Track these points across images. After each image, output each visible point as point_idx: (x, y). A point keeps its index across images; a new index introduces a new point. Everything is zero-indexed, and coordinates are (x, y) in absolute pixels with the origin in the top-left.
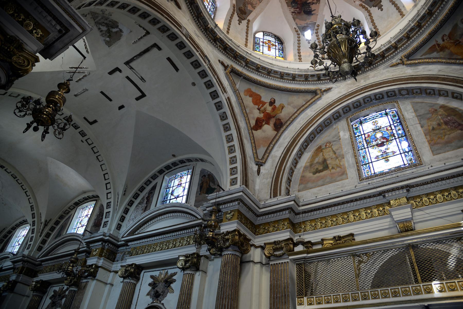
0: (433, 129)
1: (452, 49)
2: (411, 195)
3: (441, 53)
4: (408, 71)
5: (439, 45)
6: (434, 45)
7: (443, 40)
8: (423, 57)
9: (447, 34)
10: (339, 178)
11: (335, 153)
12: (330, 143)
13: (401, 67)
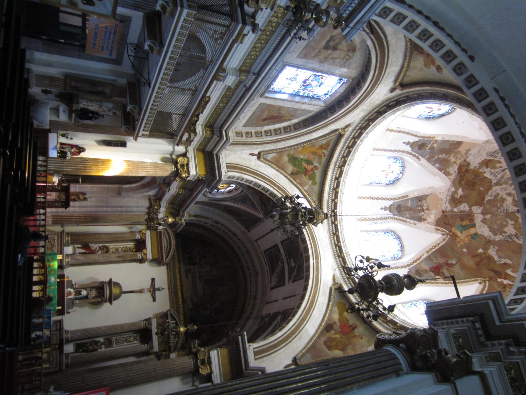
0: (280, 110)
1: (315, 149)
2: (242, 86)
3: (320, 144)
4: (332, 127)
5: (325, 149)
9: (323, 158)
10: (304, 51)
11: (332, 58)
12: (347, 59)
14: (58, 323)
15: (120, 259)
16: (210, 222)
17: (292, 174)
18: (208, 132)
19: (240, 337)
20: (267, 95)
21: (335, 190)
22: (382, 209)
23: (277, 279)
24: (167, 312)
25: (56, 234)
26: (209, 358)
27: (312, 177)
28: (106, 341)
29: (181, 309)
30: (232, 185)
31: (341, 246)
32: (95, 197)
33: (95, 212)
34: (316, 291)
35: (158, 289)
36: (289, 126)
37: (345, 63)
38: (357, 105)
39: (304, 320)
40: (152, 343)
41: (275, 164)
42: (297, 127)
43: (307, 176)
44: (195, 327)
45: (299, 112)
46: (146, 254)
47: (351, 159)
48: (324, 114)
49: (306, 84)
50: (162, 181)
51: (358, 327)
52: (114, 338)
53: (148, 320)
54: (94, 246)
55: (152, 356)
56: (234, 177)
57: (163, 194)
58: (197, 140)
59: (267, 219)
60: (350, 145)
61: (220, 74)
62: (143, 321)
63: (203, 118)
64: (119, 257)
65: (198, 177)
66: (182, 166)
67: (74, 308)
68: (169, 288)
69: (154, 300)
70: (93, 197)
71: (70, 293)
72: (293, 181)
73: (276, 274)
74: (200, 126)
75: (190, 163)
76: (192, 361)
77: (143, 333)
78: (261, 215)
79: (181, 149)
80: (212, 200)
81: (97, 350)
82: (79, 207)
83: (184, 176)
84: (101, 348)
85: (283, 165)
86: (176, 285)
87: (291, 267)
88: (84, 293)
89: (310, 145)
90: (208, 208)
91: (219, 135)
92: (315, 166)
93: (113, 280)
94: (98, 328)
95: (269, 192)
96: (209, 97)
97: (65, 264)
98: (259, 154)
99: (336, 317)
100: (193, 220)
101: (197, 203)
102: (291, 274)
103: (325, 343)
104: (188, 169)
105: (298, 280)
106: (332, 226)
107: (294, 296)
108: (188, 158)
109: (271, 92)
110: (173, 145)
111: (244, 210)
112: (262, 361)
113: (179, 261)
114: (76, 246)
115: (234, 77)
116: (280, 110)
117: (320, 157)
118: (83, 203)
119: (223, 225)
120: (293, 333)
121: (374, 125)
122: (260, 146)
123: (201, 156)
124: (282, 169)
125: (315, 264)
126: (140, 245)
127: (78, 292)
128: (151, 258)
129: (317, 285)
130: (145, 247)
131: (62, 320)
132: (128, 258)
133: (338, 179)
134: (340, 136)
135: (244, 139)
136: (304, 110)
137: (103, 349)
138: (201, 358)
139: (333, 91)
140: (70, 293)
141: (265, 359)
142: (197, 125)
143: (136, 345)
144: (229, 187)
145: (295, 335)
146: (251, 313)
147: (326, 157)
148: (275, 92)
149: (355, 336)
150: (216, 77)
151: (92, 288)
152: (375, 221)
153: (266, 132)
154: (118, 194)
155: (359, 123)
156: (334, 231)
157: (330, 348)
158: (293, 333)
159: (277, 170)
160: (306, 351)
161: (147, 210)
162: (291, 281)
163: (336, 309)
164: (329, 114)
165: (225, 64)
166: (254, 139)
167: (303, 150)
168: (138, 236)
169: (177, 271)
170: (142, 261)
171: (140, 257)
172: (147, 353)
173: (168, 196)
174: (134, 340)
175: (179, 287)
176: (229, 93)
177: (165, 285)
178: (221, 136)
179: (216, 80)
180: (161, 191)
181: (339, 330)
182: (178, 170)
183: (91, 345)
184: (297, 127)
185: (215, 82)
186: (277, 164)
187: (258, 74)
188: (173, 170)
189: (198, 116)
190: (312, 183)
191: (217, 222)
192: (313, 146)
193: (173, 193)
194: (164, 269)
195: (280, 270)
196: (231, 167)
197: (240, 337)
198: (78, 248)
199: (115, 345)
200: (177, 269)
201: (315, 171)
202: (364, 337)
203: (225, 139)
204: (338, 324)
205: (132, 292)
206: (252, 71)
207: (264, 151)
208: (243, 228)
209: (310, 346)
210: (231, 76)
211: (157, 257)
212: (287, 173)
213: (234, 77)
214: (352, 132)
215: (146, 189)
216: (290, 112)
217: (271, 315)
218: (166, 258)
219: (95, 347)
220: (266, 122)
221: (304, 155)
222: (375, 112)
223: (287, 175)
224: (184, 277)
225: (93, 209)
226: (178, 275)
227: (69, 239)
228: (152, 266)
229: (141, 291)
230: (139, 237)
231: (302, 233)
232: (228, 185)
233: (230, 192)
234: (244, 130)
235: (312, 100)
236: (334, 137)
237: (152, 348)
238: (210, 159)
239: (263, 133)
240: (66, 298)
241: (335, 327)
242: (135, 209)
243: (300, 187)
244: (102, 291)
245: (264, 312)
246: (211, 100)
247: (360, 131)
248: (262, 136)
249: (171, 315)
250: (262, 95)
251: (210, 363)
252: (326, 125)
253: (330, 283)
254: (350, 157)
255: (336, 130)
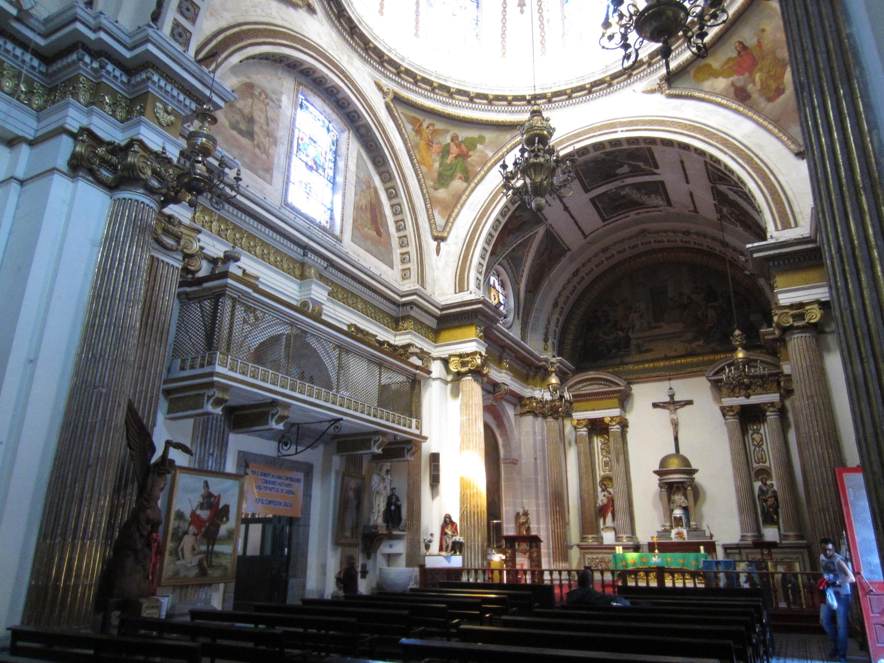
0: (361, 208)
1: (423, 143)
2: (326, 274)
3: (414, 134)
4: (383, 115)
5: (421, 125)
6: (419, 120)
7: (427, 127)
8: (402, 116)
9: (436, 127)
13: (379, 95)
14: (728, 551)
15: (621, 458)
16: (556, 316)
17: (467, 179)
18: (406, 325)
19: (755, 255)
20: (337, 232)
21: (492, 100)
22: (522, 12)
23: (653, 196)
24: (710, 381)
25: (584, 557)
26: (791, 306)
27: (471, 144)
28: (760, 477)
29: (706, 358)
30: (492, 282)
31: (591, 83)
32: (522, 498)
33: (546, 499)
34: (673, 124)
35: (672, 396)
36: (387, 190)
37: (273, 102)
38: (343, 72)
39: (726, 143)
40: (765, 404)
41: (453, 211)
42: (386, 177)
43: (470, 153)
44: (737, 332)
45: (362, 175)
46: (612, 418)
47: (436, 77)
48: (363, 131)
49: (315, 167)
50: (490, 396)
51: (741, 40)
52: (755, 465)
53: (725, 411)
54: (602, 499)
55: (788, 403)
56: (478, 279)
57: (512, 393)
58: (420, 343)
59: (546, 220)
60: (411, 80)
61: (310, 311)
62: (725, 419)
63: (383, 334)
64: (618, 460)
65: (480, 338)
66: (463, 364)
67: (705, 527)
68: (670, 379)
69: (690, 403)
70: (522, 503)
71: (679, 534)
72: (479, 177)
73: (645, 199)
74: (398, 338)
75: (458, 352)
76: (796, 336)
77: (748, 418)
78: (541, 230)
79: (436, 368)
80: (518, 314)
81: (774, 492)
82: (538, 523)
83: (479, 361)
84: (772, 485)
85: (453, 196)
86: (664, 368)
87: (631, 172)
88: (678, 513)
89: (416, 151)
90: (531, 321)
91: (408, 308)
92: (452, 140)
93: (657, 468)
94: (738, 491)
95: (501, 218)
96: (349, 326)
97: (631, 543)
98: (436, 238)
99: (721, 83)
100: (553, 343)
101: (523, 338)
102: (643, 170)
103: (770, 100)
104: (468, 355)
105: (653, 158)
106: (555, 102)
107: (682, 162)
108: (451, 356)
109: (332, 225)
110: (431, 380)
111: (533, 260)
112: (801, 213)
113: (623, 364)
114: (602, 526)
115: (314, 287)
116: (361, 208)
117: (435, 132)
118: (532, 518)
119: (560, 294)
120: (749, 161)
121: (375, 38)
122: (423, 238)
123: (445, 335)
124: (460, 197)
125: (624, 129)
126: (597, 427)
127: (678, 522)
128: (618, 410)
129: (662, 123)
130: (601, 420)
131: (723, 545)
132: (620, 445)
133: (472, 98)
134: (397, 99)
135: (413, 266)
136: (358, 167)
137: (774, 482)
138: (791, 320)
139: (322, 117)
140: (679, 534)
141: (796, 209)
142: (396, 343)
143: (768, 430)
144: (494, 287)
145: (753, 156)
146: (714, 239)
147: (434, 122)
148: (332, 218)
149: (759, 44)
150: (317, 317)
151: (670, 501)
152: (545, 22)
153: (398, 229)
154: (516, 464)
155: (373, 66)
156: (564, 97)
157: (780, 91)
158: (749, 161)
159: (462, 207)
160: (785, 135)
161: (540, 419)
162: (656, 171)
163: (707, 84)
164: (360, 123)
165: (295, 303)
166: (412, 249)
167: (424, 164)
168: (583, 431)
169: (641, 366)
170: (624, 425)
171: (618, 426)
172: (782, 412)
173: (515, 386)
174: (758, 433)
175: (667, 363)
176: (339, 294)
177: (666, 385)
178: (411, 304)
179: (321, 315)
180: (508, 397)
181: (747, 75)
182: (470, 371)
183: (766, 501)
184: (386, 177)
185: (323, 317)
186: (451, 208)
187: (305, 248)
188: (470, 378)
189: (382, 343)
190: (481, 144)
191: (555, 305)
192: (416, 146)
193: (509, 378)
194: (636, 389)
195: (635, 191)
196: (461, 286)
197: (755, 255)
198: (604, 523)
199: (767, 464)
200: (636, 367)
201: (460, 139)
202: (762, 27)
203: (415, 297)
204: (735, 78)
205: (676, 439)
206: (301, 258)
207: (432, 231)
208: (564, 260)
209: (775, 127)
210: (313, 292)
211: (616, 401)
212: (466, 189)
213: (314, 287)
214: (390, 78)
215: (505, 421)
216: (362, 191)
217: (716, 202)
218: (618, 385)
219: (770, 494)
220: (382, 230)
221: (434, 161)
222: (352, 38)
223: (470, 189)
224: (649, 356)
225: (541, 501)
226: (647, 365)
227: (590, 536)
228: (632, 408)
229: (675, 424)
230: (585, 429)
231: (569, 156)
232: (492, 289)
233: (503, 285)
234: (398, 266)
235: (339, 154)
236: (399, 111)
237: (772, 404)
238: (450, 320)
239: (402, 234)
240: (687, 540)
241: (739, 84)
242: (539, 438)
243: (489, 164)
244: (675, 485)
245: (713, 215)
246: (354, 322)
247: (386, 65)
248: (405, 236)
249: (716, 374)
250: (339, 240)
251: (801, 305)
252: (380, 124)
253: (659, 97)
254: (433, 79)
255: (388, 107)
